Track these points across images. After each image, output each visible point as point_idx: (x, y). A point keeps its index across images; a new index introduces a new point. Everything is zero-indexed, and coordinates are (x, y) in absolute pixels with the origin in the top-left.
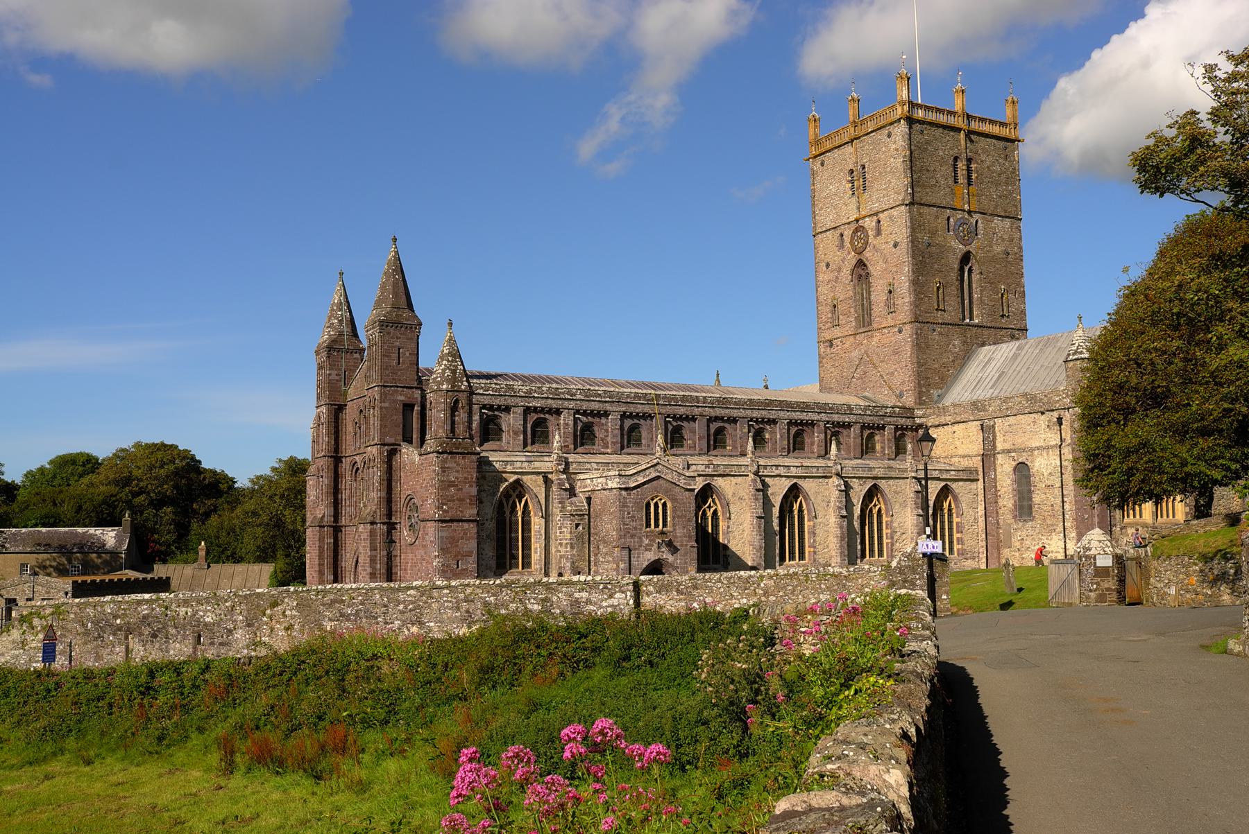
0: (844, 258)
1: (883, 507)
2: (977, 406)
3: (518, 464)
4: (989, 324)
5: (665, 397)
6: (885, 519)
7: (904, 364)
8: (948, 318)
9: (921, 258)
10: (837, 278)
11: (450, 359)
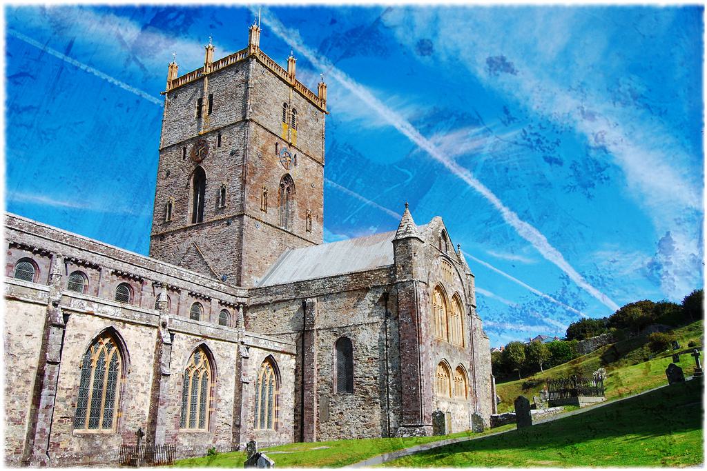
1: (209, 371)
2: (299, 285)
6: (209, 384)
7: (229, 251)
10: (175, 182)
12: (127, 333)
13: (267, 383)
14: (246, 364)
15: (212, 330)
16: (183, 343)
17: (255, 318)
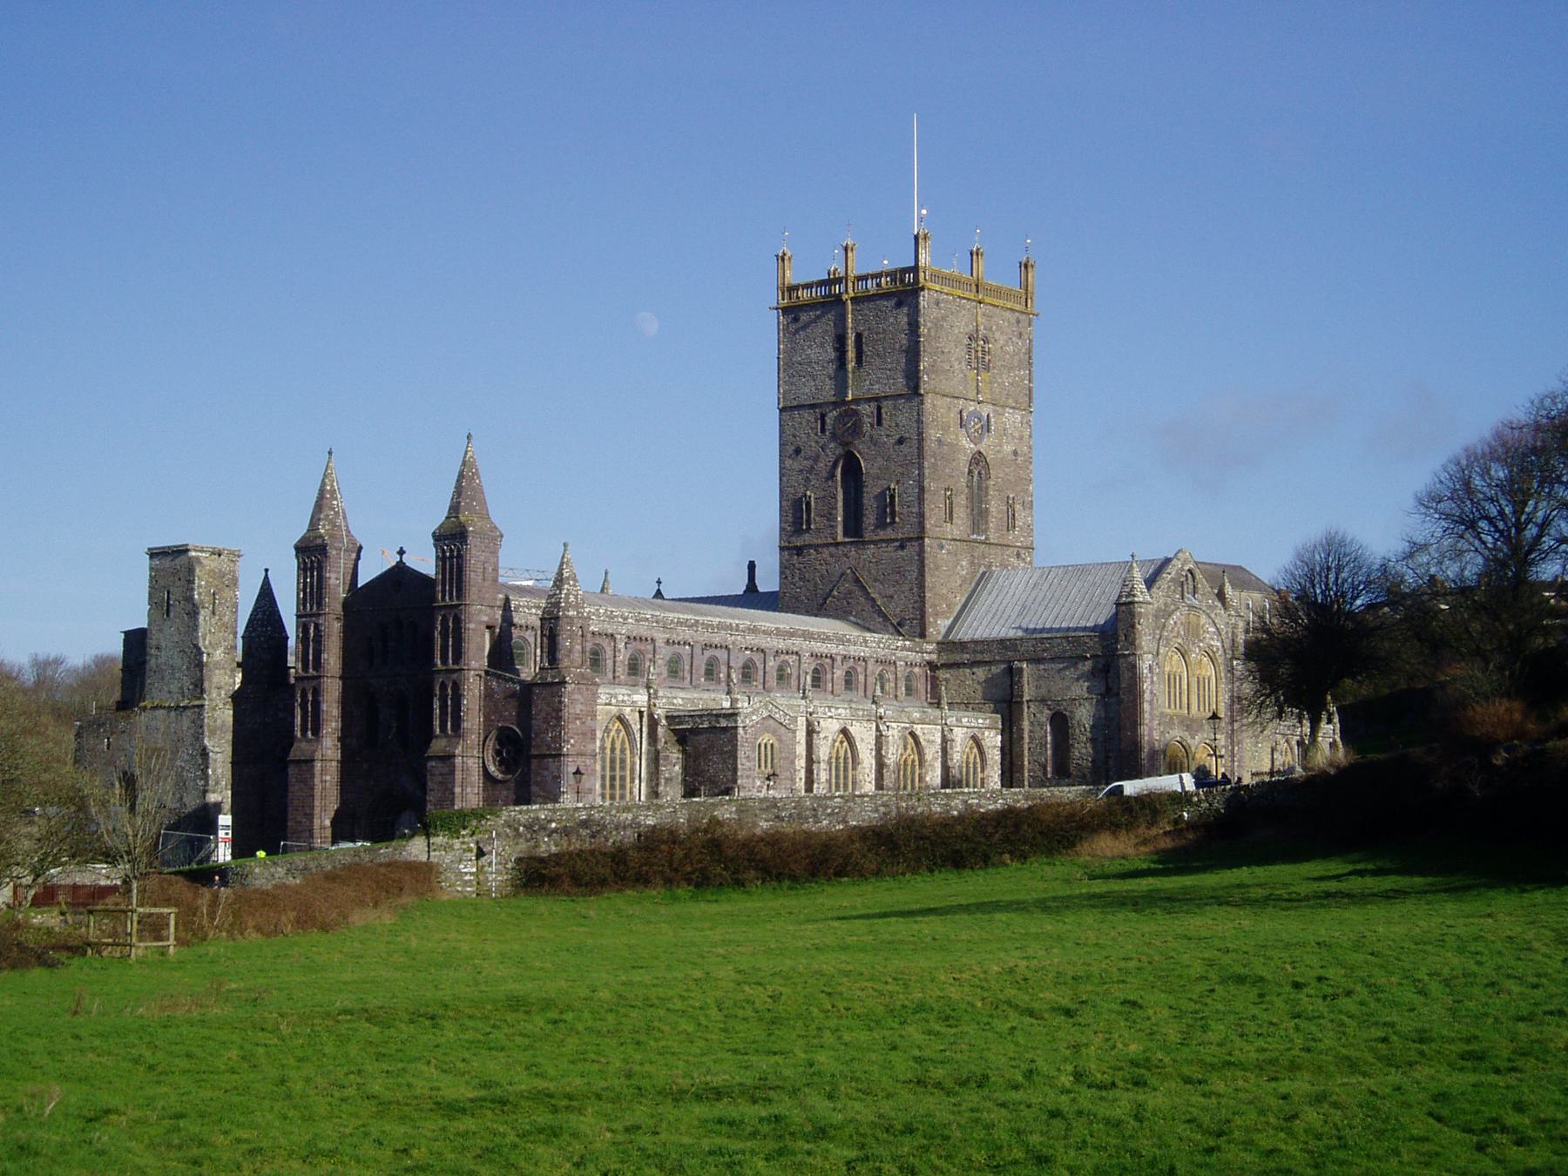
0: (824, 445)
3: (620, 698)
4: (996, 541)
5: (703, 624)
8: (957, 534)
9: (933, 460)
10: (812, 468)
11: (571, 583)
12: (854, 730)
13: (971, 765)
14: (951, 748)
15: (918, 715)
16: (895, 732)
17: (947, 680)
